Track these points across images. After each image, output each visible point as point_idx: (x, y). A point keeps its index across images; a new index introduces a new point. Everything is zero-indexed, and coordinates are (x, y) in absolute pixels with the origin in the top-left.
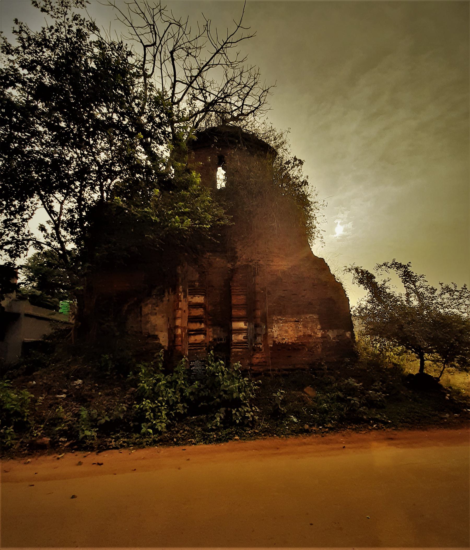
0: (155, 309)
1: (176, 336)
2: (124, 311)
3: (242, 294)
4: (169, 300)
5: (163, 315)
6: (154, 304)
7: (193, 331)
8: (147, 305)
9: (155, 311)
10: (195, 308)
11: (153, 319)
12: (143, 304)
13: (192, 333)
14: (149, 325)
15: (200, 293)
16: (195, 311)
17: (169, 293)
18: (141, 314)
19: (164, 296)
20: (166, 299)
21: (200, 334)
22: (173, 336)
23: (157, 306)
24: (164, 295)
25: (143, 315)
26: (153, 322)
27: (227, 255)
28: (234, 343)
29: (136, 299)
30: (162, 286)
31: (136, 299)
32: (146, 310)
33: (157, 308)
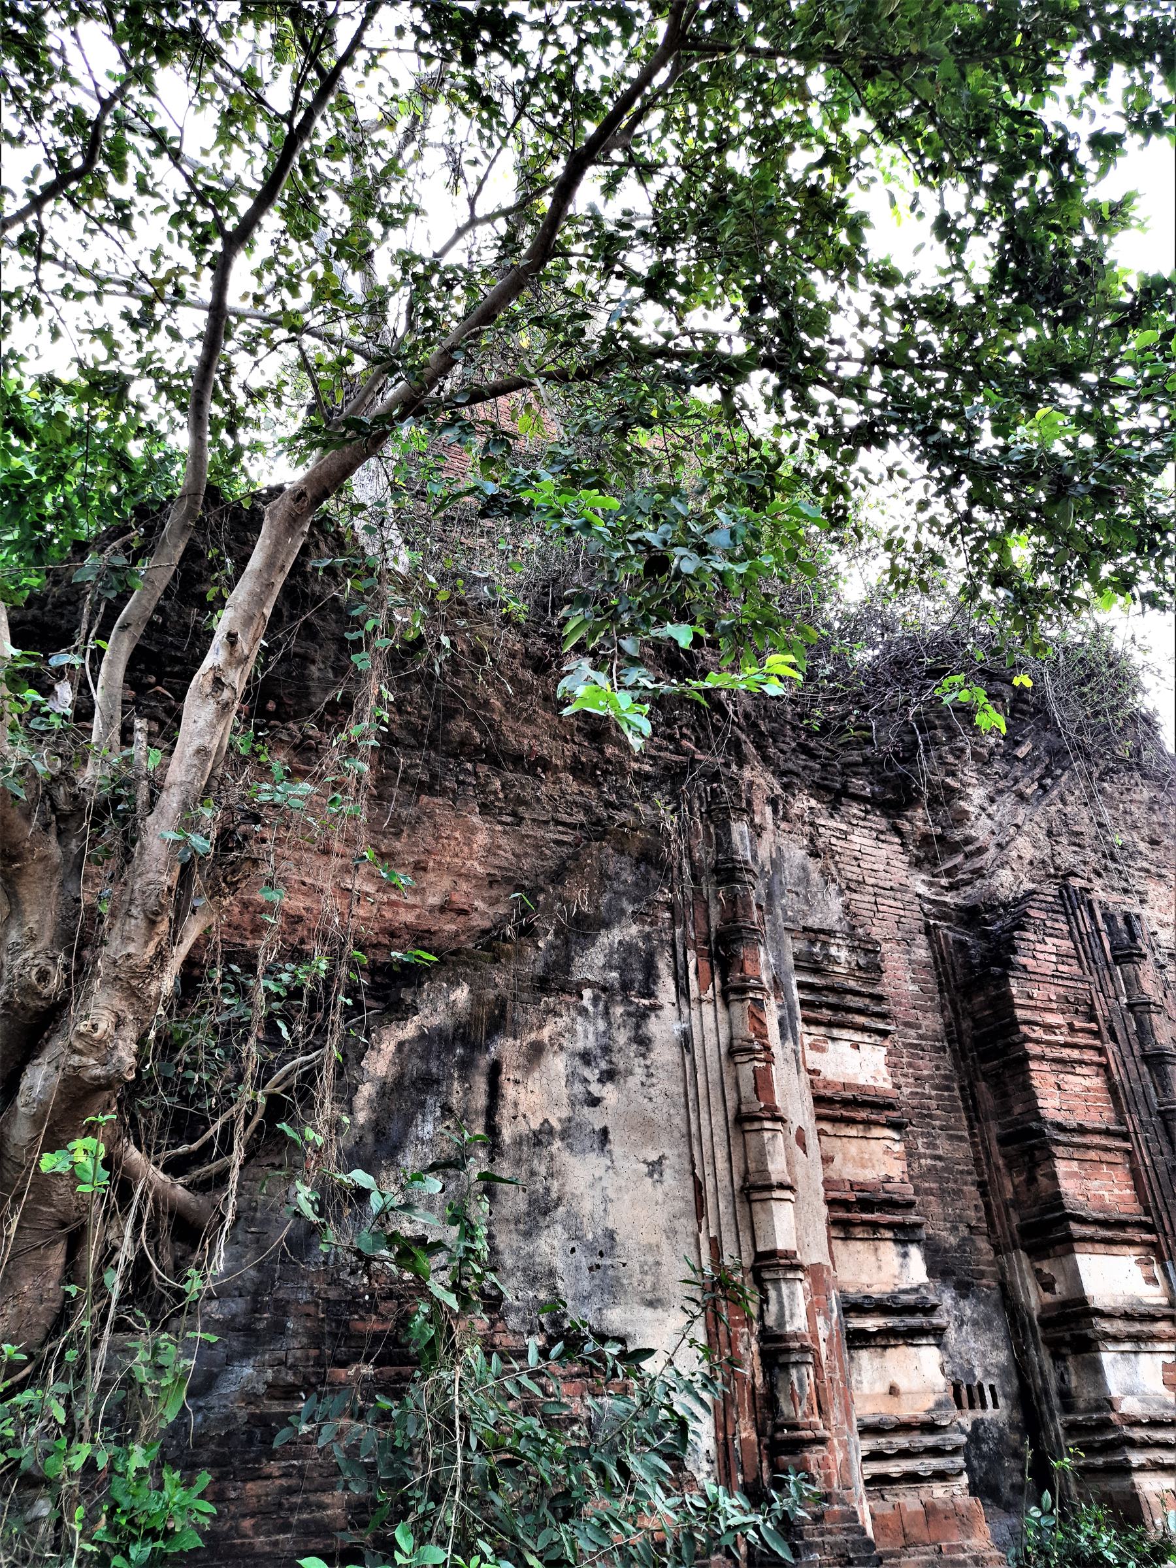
0: (594, 1102)
1: (778, 1351)
2: (367, 1091)
3: (1081, 1063)
4: (686, 1042)
5: (653, 1157)
6: (586, 1057)
7: (881, 1307)
8: (536, 1052)
9: (595, 1118)
10: (850, 1122)
11: (580, 1173)
12: (507, 1048)
13: (871, 1323)
14: (550, 1245)
15: (860, 1020)
16: (853, 1147)
17: (683, 991)
18: (492, 1130)
19: (655, 1008)
20: (664, 1027)
21: (910, 1336)
22: (749, 1349)
23: (609, 1076)
24: (650, 994)
25: (507, 1134)
26: (587, 1206)
27: (906, 827)
28: (1135, 1423)
29: (461, 995)
30: (634, 929)
31: (461, 995)
32: (536, 1097)
33: (609, 1093)
